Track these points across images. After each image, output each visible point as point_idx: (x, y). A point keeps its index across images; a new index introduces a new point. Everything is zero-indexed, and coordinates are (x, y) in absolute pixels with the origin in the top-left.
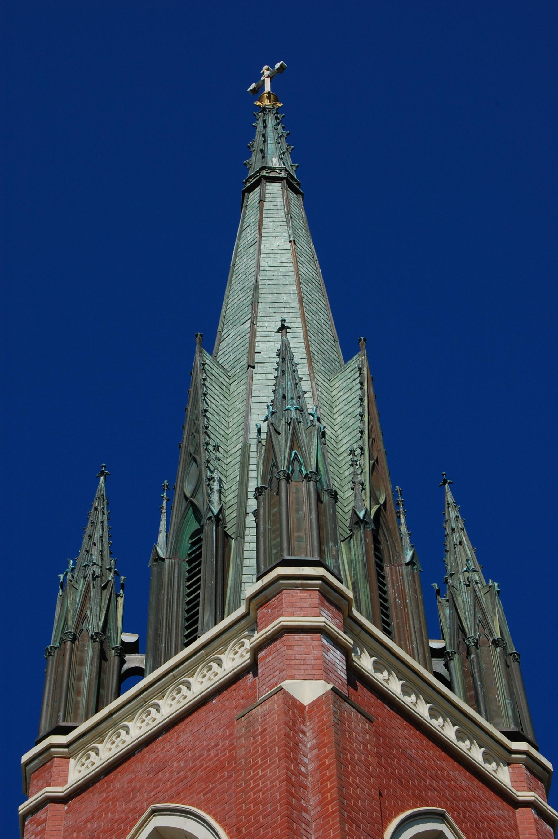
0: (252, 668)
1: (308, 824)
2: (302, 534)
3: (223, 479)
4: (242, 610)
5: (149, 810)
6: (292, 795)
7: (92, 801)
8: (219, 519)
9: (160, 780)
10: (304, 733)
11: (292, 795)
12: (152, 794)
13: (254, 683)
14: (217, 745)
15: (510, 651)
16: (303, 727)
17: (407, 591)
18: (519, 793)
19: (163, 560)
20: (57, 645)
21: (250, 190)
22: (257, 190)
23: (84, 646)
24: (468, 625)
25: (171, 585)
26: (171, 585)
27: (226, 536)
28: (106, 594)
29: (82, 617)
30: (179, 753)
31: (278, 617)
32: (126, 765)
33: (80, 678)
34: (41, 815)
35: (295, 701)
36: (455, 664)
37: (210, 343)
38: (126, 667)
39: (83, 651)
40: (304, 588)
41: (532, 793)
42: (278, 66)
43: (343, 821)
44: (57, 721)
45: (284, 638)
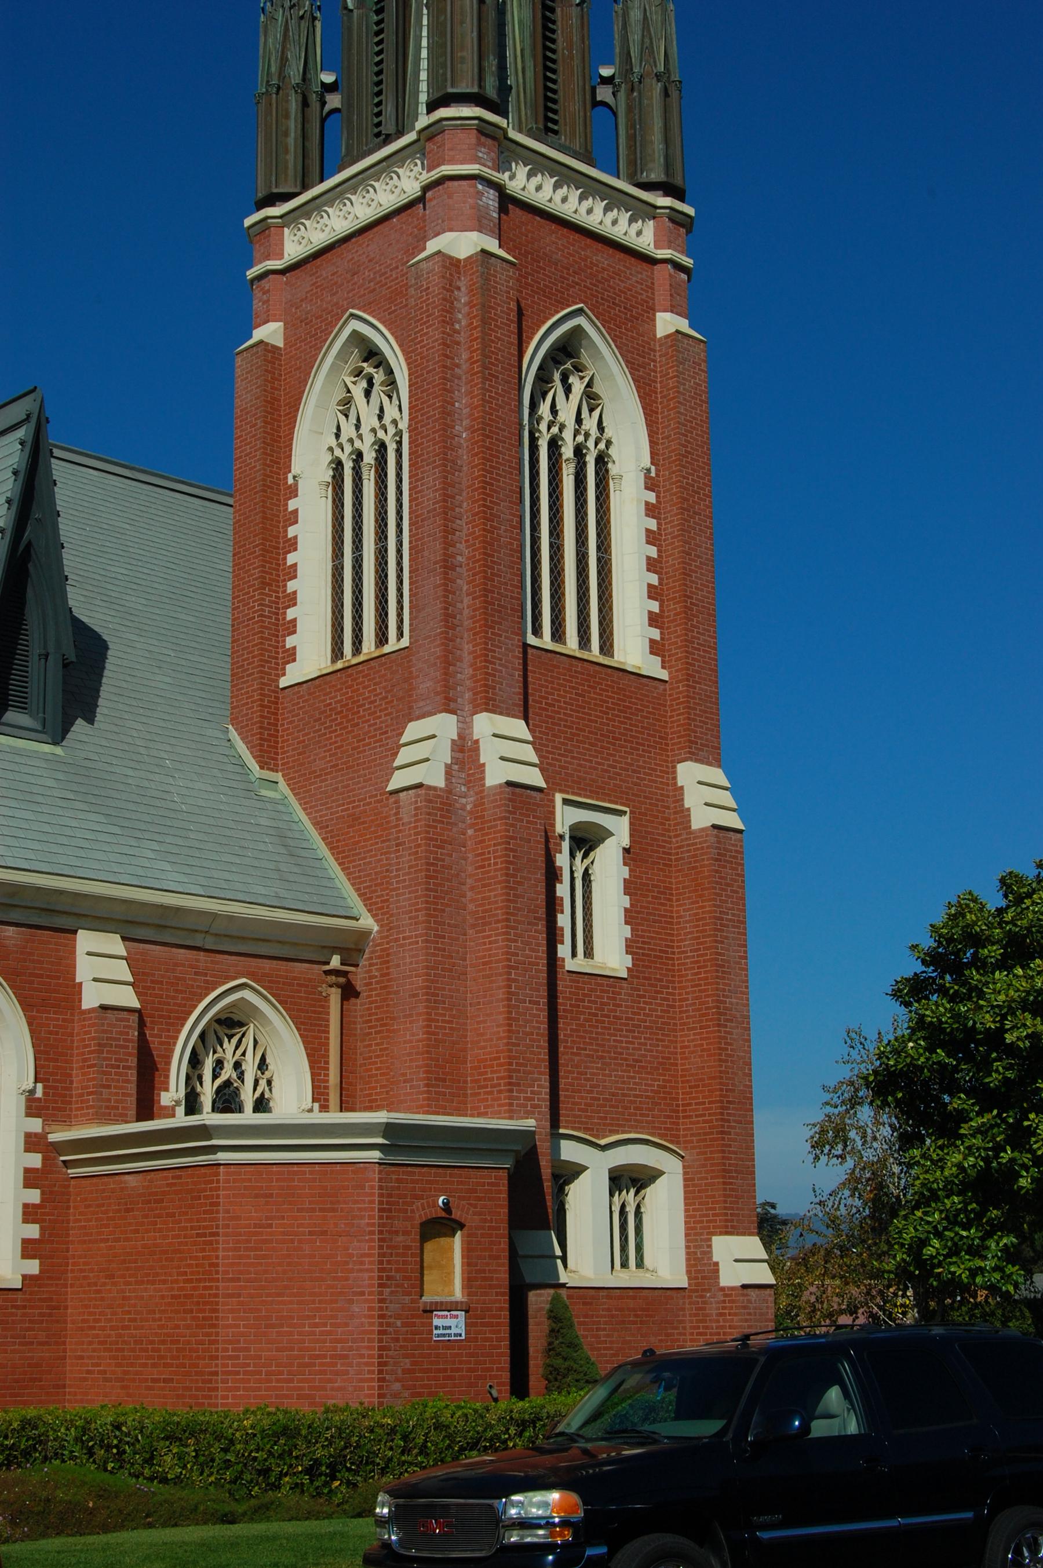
0: (421, 200)
1: (459, 378)
2: (465, 54)
5: (348, 313)
6: (447, 356)
7: (304, 281)
9: (355, 284)
10: (459, 289)
11: (447, 356)
12: (350, 295)
13: (424, 215)
14: (397, 267)
15: (673, 78)
16: (458, 283)
17: (575, 39)
18: (659, 251)
19: (351, 11)
20: (264, 90)
23: (287, 95)
24: (634, 53)
25: (360, 37)
26: (359, 42)
28: (304, 24)
29: (284, 61)
30: (370, 261)
31: (438, 165)
32: (329, 255)
33: (286, 134)
34: (265, 284)
35: (451, 258)
36: (622, 95)
38: (327, 108)
39: (287, 101)
40: (463, 128)
41: (670, 251)
43: (485, 379)
44: (270, 187)
45: (446, 185)
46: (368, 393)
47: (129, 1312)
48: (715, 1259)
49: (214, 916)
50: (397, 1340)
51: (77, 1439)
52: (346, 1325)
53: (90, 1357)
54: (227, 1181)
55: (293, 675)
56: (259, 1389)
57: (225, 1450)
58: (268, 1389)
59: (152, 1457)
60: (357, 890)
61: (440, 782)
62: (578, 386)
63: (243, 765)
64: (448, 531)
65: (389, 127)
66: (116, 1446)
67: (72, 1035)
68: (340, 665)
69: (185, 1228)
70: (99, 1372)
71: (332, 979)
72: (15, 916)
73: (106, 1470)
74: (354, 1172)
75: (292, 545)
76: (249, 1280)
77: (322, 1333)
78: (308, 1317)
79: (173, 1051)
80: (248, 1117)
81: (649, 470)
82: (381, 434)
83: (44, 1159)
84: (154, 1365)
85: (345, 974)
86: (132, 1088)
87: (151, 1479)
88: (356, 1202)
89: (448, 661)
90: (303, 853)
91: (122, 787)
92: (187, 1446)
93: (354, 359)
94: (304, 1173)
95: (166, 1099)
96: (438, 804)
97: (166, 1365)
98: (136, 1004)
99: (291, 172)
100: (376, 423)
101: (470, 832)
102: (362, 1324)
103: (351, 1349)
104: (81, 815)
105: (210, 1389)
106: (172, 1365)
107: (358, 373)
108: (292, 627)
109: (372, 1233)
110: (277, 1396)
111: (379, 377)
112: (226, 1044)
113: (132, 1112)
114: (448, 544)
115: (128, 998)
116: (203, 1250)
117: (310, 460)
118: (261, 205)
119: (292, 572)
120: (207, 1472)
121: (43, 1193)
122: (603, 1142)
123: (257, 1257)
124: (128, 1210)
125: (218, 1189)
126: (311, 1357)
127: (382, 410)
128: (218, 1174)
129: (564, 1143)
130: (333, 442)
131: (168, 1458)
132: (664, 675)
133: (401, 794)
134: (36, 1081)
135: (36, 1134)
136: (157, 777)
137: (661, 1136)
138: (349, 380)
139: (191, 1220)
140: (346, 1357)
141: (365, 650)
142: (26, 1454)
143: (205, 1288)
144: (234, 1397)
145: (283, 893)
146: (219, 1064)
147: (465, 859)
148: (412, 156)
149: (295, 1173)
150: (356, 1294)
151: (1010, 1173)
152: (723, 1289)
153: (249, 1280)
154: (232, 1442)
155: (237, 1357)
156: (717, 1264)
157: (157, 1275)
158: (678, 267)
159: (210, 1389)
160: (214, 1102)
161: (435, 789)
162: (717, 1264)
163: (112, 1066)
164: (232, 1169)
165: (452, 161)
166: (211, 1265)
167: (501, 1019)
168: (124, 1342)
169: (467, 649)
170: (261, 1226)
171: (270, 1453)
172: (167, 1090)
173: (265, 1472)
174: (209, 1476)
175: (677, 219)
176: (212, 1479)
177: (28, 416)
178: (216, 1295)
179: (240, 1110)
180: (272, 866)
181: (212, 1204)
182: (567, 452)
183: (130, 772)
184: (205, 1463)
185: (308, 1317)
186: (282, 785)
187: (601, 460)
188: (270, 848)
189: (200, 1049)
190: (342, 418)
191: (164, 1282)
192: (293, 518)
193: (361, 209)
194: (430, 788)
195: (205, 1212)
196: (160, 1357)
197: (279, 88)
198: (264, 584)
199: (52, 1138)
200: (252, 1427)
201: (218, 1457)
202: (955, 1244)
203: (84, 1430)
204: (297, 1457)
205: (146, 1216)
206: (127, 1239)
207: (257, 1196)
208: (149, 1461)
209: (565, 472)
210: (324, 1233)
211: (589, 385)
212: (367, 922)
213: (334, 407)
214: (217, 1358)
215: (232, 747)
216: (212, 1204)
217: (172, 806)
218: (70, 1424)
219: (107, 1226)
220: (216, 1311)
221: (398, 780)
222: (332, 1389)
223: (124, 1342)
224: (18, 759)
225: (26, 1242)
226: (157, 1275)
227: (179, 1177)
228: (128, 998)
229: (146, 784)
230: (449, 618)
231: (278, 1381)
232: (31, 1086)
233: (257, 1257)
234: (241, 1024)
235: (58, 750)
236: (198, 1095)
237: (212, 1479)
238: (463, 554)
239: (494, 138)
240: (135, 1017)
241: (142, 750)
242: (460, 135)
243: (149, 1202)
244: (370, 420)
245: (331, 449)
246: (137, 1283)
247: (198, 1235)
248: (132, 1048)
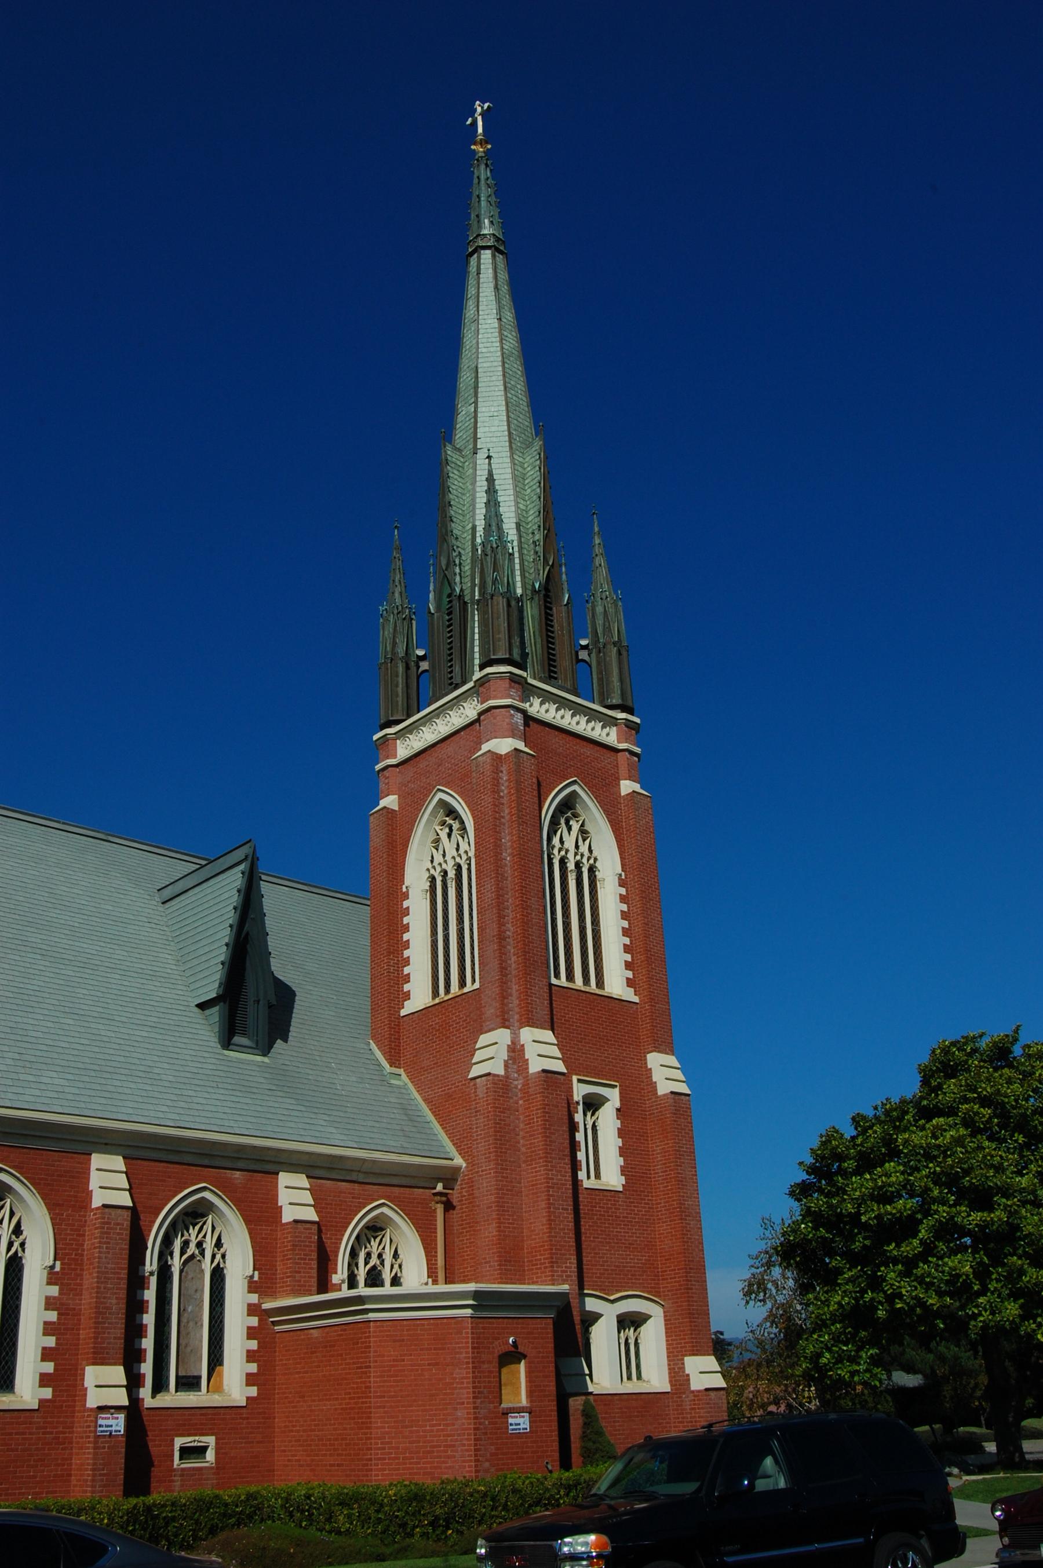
0: (477, 721)
3: (462, 552)
4: (471, 684)
7: (410, 770)
8: (461, 597)
21: (471, 254)
22: (475, 255)
24: (600, 631)
27: (465, 603)
29: (394, 644)
33: (397, 686)
36: (593, 655)
37: (448, 436)
38: (421, 670)
42: (486, 105)
46: (449, 835)
47: (314, 1420)
48: (687, 1372)
49: (364, 1161)
50: (486, 1434)
51: (283, 1506)
52: (453, 1425)
53: (290, 1451)
54: (375, 1332)
55: (409, 1008)
56: (398, 1469)
57: (378, 1511)
58: (404, 1469)
59: (331, 1517)
60: (452, 1141)
61: (501, 1071)
62: (575, 826)
63: (380, 1065)
64: (501, 917)
65: (457, 679)
66: (308, 1511)
67: (276, 1239)
68: (437, 1001)
69: (349, 1364)
70: (297, 1461)
71: (438, 1198)
72: (240, 1164)
73: (301, 1526)
74: (455, 1323)
75: (406, 928)
76: (390, 1397)
77: (438, 1431)
78: (429, 1420)
79: (339, 1248)
80: (387, 1289)
81: (620, 875)
82: (458, 860)
83: (260, 1321)
84: (331, 1455)
85: (446, 1195)
86: (314, 1273)
87: (330, 1532)
88: (457, 1343)
89: (504, 996)
90: (419, 1119)
91: (306, 1081)
92: (353, 1509)
93: (441, 815)
94: (423, 1325)
95: (336, 1279)
96: (500, 1085)
97: (338, 1455)
98: (317, 1219)
99: (400, 708)
100: (455, 854)
101: (521, 1102)
102: (463, 1424)
103: (456, 1440)
104: (280, 1100)
105: (367, 1470)
106: (342, 1455)
107: (443, 823)
108: (407, 979)
109: (468, 1363)
110: (410, 1474)
111: (456, 825)
112: (372, 1243)
113: (315, 1289)
114: (501, 924)
115: (311, 1215)
116: (361, 1378)
118: (383, 727)
119: (407, 945)
120: (366, 1526)
121: (259, 1343)
122: (612, 1298)
123: (394, 1381)
124: (312, 1353)
125: (369, 1337)
126: (431, 1447)
127: (458, 845)
128: (369, 1327)
129: (587, 1300)
130: (430, 866)
131: (341, 1518)
132: (636, 999)
133: (478, 1080)
134: (254, 1270)
135: (254, 1305)
136: (326, 1075)
137: (649, 1292)
138: (438, 828)
139: (353, 1358)
140: (454, 1446)
141: (452, 991)
142: (250, 1517)
143: (363, 1403)
144: (383, 1475)
145: (406, 1145)
146: (369, 1255)
147: (518, 1119)
148: (471, 696)
149: (418, 1325)
150: (458, 1403)
151: (872, 1307)
152: (693, 1392)
153: (390, 1397)
154: (382, 1505)
155: (384, 1449)
156: (688, 1375)
157: (332, 1395)
158: (632, 753)
159: (367, 1470)
160: (366, 1280)
161: (498, 1076)
162: (688, 1375)
163: (301, 1259)
164: (378, 1324)
165: (495, 698)
166: (366, 1387)
167: (544, 1221)
168: (312, 1440)
169: (514, 988)
170: (397, 1361)
171: (407, 1513)
172: (336, 1273)
173: (403, 1525)
174: (369, 1528)
176: (369, 1531)
177: (246, 857)
178: (370, 1407)
179: (382, 1285)
180: (398, 1127)
181: (366, 1347)
182: (571, 866)
183: (311, 1072)
184: (364, 1520)
185: (429, 1420)
186: (404, 1077)
187: (592, 870)
188: (398, 1116)
189: (357, 1246)
190: (434, 851)
191: (337, 1399)
192: (406, 912)
193: (442, 727)
194: (495, 1075)
195: (362, 1353)
196: (335, 1450)
197: (392, 660)
198: (389, 953)
199: (265, 1306)
200: (395, 1495)
201: (373, 1516)
202: (840, 1355)
203: (287, 1500)
204: (424, 1515)
205: (325, 1356)
206: (313, 1372)
207: (395, 1341)
208: (329, 1520)
209: (570, 879)
210: (437, 1364)
211: (582, 825)
212: (459, 1161)
213: (429, 844)
214: (371, 1449)
215: (373, 1054)
216: (366, 1347)
217: (336, 1092)
218: (277, 1496)
219: (300, 1363)
220: (370, 1418)
221: (475, 1071)
222: (446, 1468)
223: (312, 1440)
224: (241, 1066)
225: (249, 1375)
226: (332, 1395)
227: (345, 1330)
228: (311, 1215)
229: (320, 1079)
230: (503, 969)
231: (411, 1463)
232: (251, 1273)
233: (394, 1381)
234: (382, 1229)
235: (266, 1060)
236: (356, 1276)
237: (369, 1531)
238: (510, 929)
239: (519, 683)
240: (315, 1227)
241: (318, 1058)
242: (500, 682)
243: (326, 1347)
244: (451, 852)
245: (428, 870)
246: (319, 1400)
247: (358, 1368)
248: (314, 1247)
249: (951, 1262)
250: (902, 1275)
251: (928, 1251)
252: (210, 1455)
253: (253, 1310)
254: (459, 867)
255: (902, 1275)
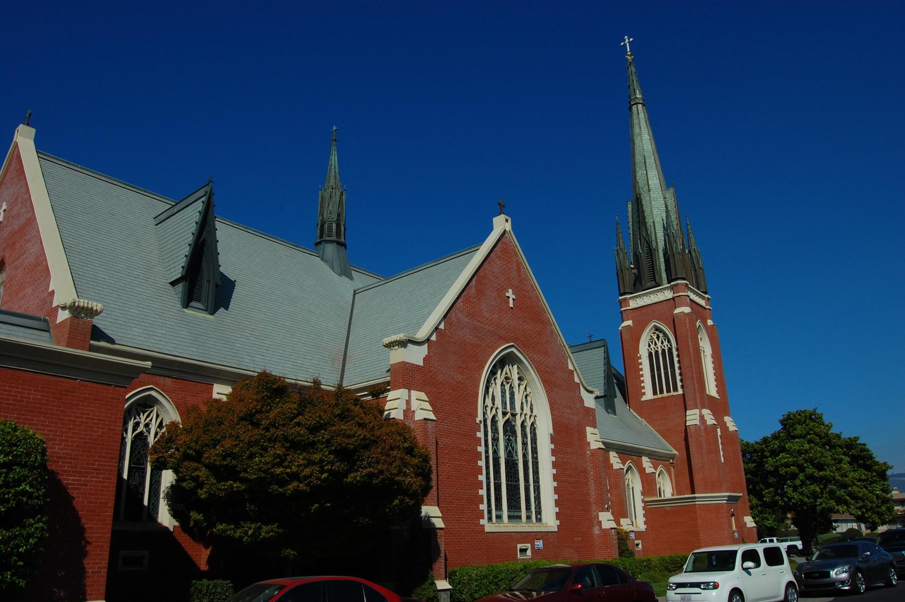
55: (644, 398)
93: (653, 331)
111: (661, 335)
117: (643, 351)
151: (777, 501)
175: (708, 299)
212: (675, 452)
244: (659, 344)
249: (812, 487)
250: (794, 491)
251: (803, 483)
252: (640, 546)
253: (643, 501)
254: (663, 351)
255: (794, 491)
